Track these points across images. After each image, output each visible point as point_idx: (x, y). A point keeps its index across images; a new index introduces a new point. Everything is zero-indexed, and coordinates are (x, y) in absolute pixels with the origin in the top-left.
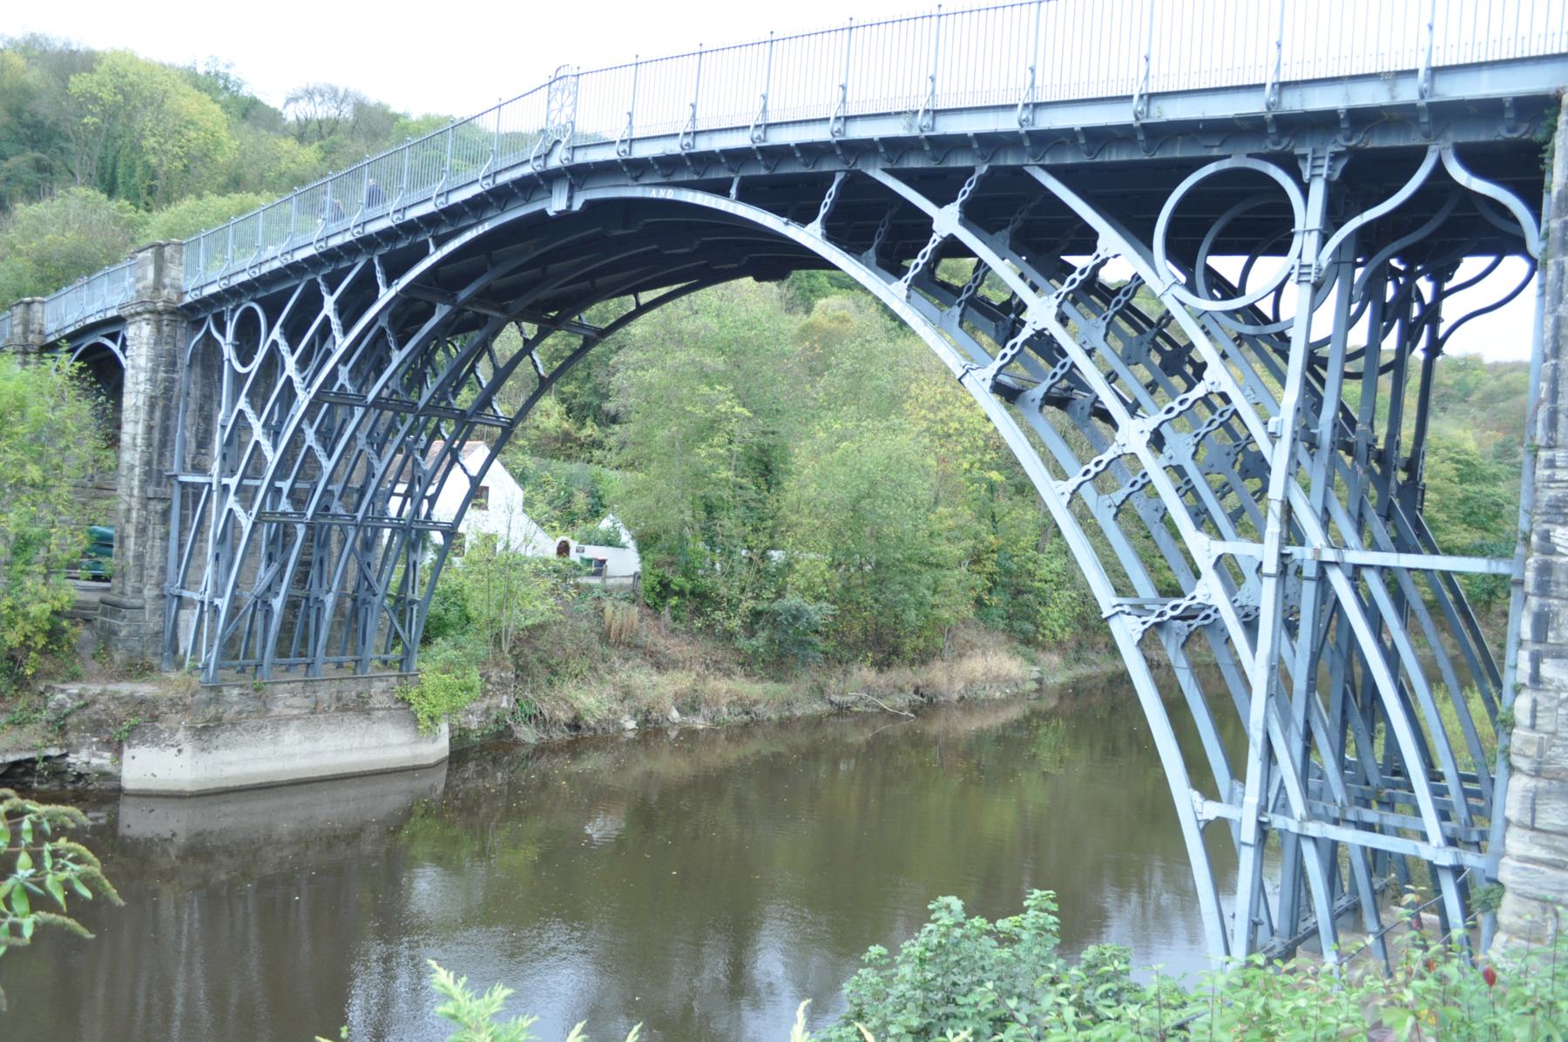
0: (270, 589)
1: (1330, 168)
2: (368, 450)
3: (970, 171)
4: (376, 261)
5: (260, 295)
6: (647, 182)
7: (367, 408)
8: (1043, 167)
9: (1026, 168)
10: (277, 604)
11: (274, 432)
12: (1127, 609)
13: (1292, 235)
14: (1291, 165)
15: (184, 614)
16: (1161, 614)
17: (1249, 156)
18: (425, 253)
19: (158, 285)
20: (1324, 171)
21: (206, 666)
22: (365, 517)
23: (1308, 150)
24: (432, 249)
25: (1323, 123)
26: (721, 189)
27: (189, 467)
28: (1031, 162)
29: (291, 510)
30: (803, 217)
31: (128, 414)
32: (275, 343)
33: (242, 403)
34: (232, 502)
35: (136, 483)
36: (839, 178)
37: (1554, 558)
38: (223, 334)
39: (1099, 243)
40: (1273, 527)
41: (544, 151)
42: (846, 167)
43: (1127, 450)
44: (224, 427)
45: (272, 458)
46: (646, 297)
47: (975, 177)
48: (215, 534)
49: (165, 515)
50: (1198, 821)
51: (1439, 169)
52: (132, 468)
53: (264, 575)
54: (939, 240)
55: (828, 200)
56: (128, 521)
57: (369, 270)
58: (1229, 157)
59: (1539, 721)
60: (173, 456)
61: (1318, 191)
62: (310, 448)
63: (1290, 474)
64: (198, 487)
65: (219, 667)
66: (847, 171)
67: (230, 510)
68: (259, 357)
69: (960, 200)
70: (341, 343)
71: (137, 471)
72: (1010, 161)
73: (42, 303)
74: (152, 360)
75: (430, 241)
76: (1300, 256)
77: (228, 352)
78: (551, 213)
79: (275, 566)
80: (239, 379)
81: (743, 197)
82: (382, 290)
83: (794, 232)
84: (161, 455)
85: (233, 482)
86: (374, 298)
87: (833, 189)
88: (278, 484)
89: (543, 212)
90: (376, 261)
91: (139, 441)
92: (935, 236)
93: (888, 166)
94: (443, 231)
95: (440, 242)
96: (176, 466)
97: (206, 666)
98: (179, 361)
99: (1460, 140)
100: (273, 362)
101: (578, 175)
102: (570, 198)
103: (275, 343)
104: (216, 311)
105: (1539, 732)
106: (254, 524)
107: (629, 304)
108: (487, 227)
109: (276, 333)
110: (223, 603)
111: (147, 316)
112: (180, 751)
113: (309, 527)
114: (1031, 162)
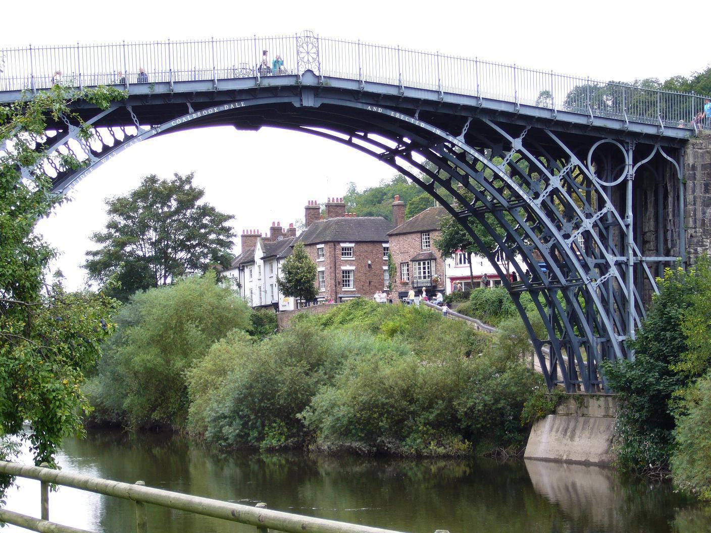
4: (130, 109)
8: (551, 131)
18: (185, 112)
24: (191, 110)
26: (411, 113)
51: (658, 152)
75: (189, 105)
78: (297, 105)
83: (451, 138)
87: (468, 123)
90: (130, 109)
92: (513, 150)
95: (198, 107)
108: (243, 104)
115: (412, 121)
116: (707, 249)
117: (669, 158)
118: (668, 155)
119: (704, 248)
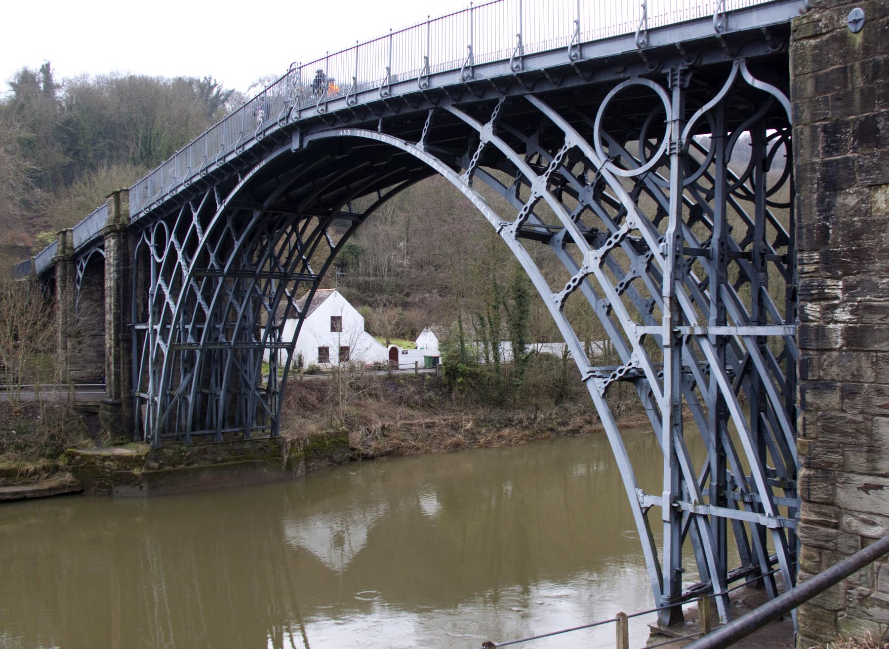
0: (188, 388)
1: (681, 80)
2: (235, 302)
3: (497, 101)
5: (165, 216)
6: (338, 126)
7: (225, 277)
8: (534, 95)
9: (526, 97)
10: (190, 398)
11: (174, 295)
12: (597, 374)
13: (666, 124)
14: (662, 81)
15: (143, 406)
16: (614, 376)
17: (640, 76)
18: (237, 183)
19: (118, 216)
20: (678, 83)
21: (153, 438)
22: (235, 343)
23: (668, 70)
24: (240, 179)
25: (668, 53)
26: (372, 127)
27: (140, 320)
28: (527, 92)
29: (193, 342)
30: (413, 139)
31: (107, 292)
32: (172, 243)
33: (160, 281)
34: (158, 340)
35: (112, 332)
36: (431, 112)
37: (808, 324)
38: (150, 240)
39: (566, 139)
40: (667, 315)
41: (286, 114)
42: (434, 106)
43: (589, 271)
44: (152, 295)
45: (174, 310)
46: (384, 192)
47: (499, 104)
48: (152, 359)
49: (129, 350)
50: (641, 509)
52: (110, 323)
53: (183, 382)
54: (483, 146)
55: (426, 127)
56: (111, 354)
57: (212, 195)
58: (629, 78)
59: (808, 432)
60: (131, 314)
61: (676, 94)
62: (199, 303)
63: (676, 279)
64: (144, 331)
65: (160, 437)
66: (435, 108)
67: (158, 344)
68: (166, 253)
69: (492, 120)
70: (202, 239)
71: (112, 324)
72: (516, 93)
73: (71, 231)
74: (117, 259)
76: (670, 138)
77: (153, 250)
79: (189, 376)
80: (159, 265)
81: (386, 131)
82: (218, 207)
83: (410, 149)
84: (124, 314)
85: (158, 327)
86: (215, 212)
87: (428, 120)
88: (187, 327)
89: (290, 150)
91: (112, 307)
92: (481, 144)
93: (455, 103)
94: (245, 167)
96: (133, 320)
97: (153, 438)
98: (131, 258)
99: (749, 56)
100: (173, 254)
101: (305, 126)
102: (301, 141)
103: (172, 242)
104: (146, 227)
105: (809, 438)
106: (169, 352)
107: (373, 197)
108: (264, 163)
109: (173, 238)
110: (158, 399)
111: (112, 234)
112: (141, 487)
113: (201, 350)
114: (527, 92)
115: (375, 136)
116: (835, 307)
117: (758, 84)
118: (756, 76)
119: (824, 303)
